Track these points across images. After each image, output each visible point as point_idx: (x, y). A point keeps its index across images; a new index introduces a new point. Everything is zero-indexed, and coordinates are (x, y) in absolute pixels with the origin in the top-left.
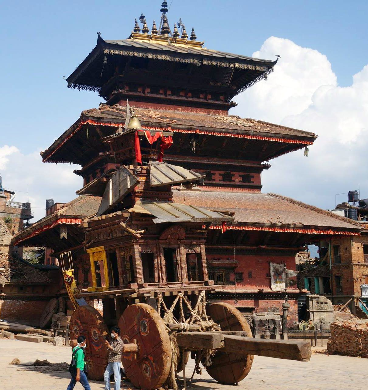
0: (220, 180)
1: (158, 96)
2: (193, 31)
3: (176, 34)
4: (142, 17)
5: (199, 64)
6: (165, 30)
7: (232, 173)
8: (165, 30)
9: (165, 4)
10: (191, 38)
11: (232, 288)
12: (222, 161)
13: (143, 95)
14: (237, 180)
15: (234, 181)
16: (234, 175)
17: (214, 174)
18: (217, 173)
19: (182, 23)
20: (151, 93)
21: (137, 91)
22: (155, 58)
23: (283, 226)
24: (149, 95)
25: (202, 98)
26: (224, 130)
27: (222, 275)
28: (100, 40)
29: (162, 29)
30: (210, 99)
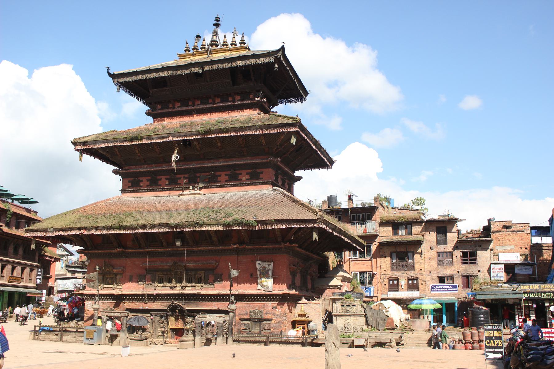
0: (226, 181)
3: (225, 44)
5: (200, 71)
7: (238, 172)
8: (214, 43)
9: (217, 19)
10: (240, 43)
11: (208, 290)
12: (227, 161)
14: (244, 178)
15: (241, 180)
16: (241, 174)
17: (220, 176)
18: (223, 174)
20: (182, 106)
21: (168, 108)
23: (263, 222)
24: (180, 109)
25: (231, 101)
26: (195, 133)
29: (211, 41)
30: (238, 100)
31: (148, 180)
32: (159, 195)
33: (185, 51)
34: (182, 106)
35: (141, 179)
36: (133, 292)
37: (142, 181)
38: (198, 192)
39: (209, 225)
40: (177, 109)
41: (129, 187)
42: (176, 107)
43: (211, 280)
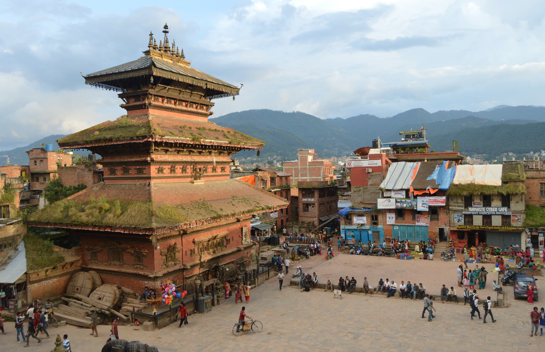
2: (182, 51)
5: (205, 88)
9: (166, 27)
13: (162, 105)
21: (158, 101)
32: (176, 181)
33: (149, 47)
35: (164, 167)
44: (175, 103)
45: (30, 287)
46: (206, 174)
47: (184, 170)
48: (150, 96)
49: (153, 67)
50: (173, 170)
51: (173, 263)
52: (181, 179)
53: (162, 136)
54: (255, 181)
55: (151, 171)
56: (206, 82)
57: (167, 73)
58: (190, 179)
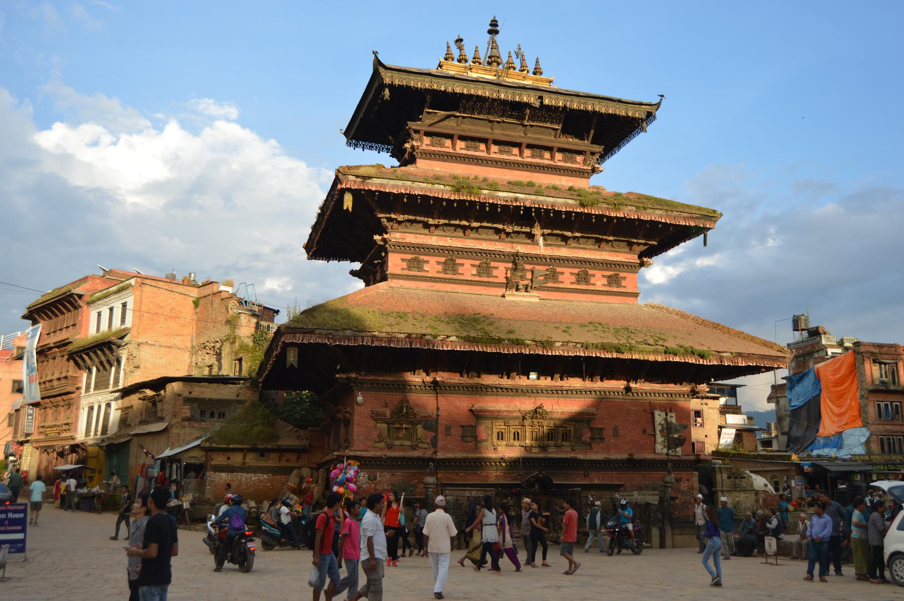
0: (572, 283)
1: (477, 154)
2: (537, 62)
3: (510, 66)
4: (459, 40)
6: (493, 60)
7: (590, 272)
8: (493, 60)
9: (494, 23)
13: (451, 151)
14: (599, 283)
15: (594, 284)
16: (594, 275)
17: (562, 273)
18: (567, 271)
19: (522, 51)
21: (442, 146)
22: (465, 92)
27: (570, 431)
28: (378, 63)
29: (490, 57)
31: (438, 263)
34: (467, 148)
35: (425, 258)
36: (459, 455)
37: (427, 262)
38: (535, 293)
39: (640, 352)
40: (458, 151)
41: (403, 269)
42: (458, 148)
43: (587, 436)
44: (488, 149)
45: (211, 475)
46: (555, 285)
47: (484, 269)
48: (415, 136)
49: (381, 69)
50: (450, 265)
51: (407, 443)
52: (474, 288)
53: (365, 178)
54: (854, 365)
55: (390, 264)
56: (539, 94)
57: (420, 78)
58: (502, 291)
